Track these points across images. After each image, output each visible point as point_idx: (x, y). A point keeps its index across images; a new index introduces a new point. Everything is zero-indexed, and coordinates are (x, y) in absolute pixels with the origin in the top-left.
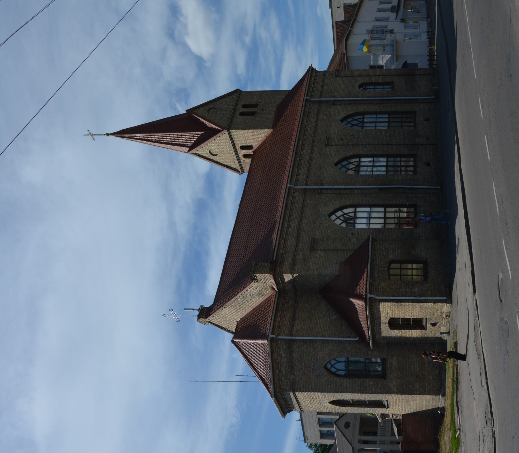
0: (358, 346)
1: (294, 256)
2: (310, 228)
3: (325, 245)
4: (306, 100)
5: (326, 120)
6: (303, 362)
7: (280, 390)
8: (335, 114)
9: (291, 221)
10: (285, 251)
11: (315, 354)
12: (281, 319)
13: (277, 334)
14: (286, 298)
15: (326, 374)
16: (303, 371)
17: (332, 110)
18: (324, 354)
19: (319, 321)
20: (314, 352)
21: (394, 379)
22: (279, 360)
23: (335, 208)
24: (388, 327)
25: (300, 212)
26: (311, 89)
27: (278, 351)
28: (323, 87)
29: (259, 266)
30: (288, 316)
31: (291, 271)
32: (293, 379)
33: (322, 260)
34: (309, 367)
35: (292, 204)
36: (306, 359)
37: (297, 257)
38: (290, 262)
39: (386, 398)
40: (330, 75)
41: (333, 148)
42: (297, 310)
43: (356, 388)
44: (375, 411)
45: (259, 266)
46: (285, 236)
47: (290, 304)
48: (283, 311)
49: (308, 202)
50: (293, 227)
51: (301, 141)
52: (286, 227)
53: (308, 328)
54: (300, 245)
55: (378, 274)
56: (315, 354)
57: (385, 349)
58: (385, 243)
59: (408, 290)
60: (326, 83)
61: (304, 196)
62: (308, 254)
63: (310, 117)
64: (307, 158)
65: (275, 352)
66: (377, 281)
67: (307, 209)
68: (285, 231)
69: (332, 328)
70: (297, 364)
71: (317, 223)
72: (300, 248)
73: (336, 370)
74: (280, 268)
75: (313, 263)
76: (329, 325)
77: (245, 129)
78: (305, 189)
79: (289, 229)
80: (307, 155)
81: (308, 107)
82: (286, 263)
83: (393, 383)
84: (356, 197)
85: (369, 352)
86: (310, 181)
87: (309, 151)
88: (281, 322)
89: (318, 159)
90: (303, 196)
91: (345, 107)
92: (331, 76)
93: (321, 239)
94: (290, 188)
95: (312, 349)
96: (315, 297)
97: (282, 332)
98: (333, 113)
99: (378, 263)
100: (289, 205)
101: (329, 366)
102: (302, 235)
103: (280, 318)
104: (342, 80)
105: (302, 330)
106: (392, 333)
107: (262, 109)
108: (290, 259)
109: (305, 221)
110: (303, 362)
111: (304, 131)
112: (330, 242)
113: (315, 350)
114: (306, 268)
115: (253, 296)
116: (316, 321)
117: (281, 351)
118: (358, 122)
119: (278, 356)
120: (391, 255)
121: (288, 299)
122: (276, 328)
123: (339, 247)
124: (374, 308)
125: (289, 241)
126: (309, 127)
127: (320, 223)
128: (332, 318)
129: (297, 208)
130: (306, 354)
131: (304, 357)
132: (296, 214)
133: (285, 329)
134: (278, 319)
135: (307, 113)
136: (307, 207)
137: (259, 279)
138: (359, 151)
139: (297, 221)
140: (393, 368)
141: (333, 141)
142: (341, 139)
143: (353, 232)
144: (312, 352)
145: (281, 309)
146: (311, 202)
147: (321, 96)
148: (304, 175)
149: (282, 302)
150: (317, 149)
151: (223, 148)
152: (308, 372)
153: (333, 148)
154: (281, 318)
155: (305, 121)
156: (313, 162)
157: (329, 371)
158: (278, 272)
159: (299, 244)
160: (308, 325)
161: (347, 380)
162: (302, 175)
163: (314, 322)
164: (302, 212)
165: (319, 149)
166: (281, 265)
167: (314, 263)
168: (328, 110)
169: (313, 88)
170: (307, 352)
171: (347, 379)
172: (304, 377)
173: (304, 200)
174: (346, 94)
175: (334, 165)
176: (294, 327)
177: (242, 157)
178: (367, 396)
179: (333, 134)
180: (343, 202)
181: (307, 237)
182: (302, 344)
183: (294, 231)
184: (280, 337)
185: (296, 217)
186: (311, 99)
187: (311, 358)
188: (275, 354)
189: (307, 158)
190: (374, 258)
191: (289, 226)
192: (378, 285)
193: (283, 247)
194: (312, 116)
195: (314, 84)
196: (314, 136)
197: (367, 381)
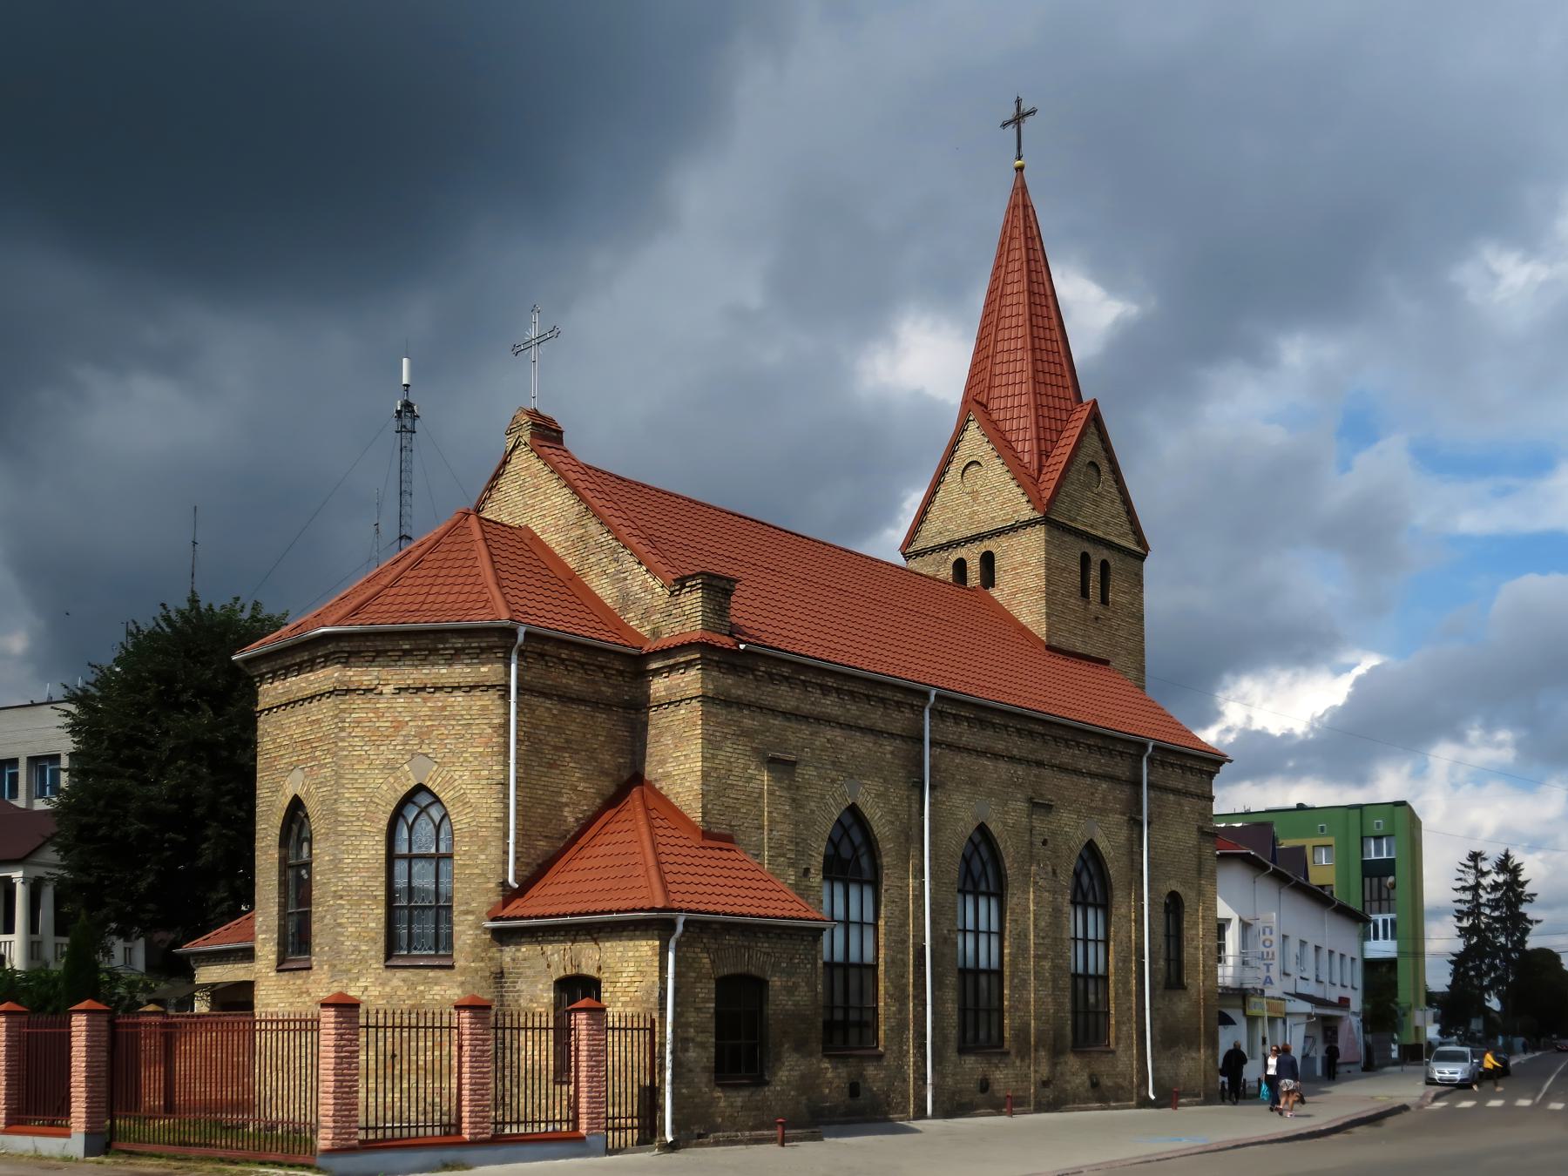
0: (492, 885)
1: (749, 705)
2: (822, 750)
3: (778, 793)
4: (1144, 746)
6: (436, 723)
7: (345, 652)
9: (839, 697)
10: (762, 676)
11: (461, 759)
12: (564, 660)
13: (523, 648)
14: (620, 679)
15: (399, 789)
16: (407, 722)
18: (464, 786)
19: (558, 772)
20: (468, 755)
21: (388, 989)
22: (441, 652)
23: (872, 823)
24: (562, 973)
25: (861, 723)
27: (471, 651)
28: (1176, 792)
29: (722, 600)
30: (572, 683)
31: (710, 695)
32: (381, 693)
33: (740, 783)
34: (422, 742)
36: (446, 732)
37: (745, 712)
38: (733, 691)
39: (321, 967)
42: (588, 709)
43: (354, 879)
44: (265, 932)
45: (722, 600)
46: (802, 677)
47: (603, 688)
48: (586, 667)
49: (888, 748)
50: (823, 701)
51: (1040, 729)
52: (824, 682)
53: (540, 740)
54: (776, 722)
55: (732, 947)
56: (461, 759)
57: (482, 964)
58: (809, 966)
59: (692, 1030)
61: (901, 736)
62: (754, 745)
63: (1101, 755)
65: (470, 640)
66: (713, 941)
68: (814, 680)
69: (539, 811)
70: (429, 704)
71: (834, 773)
72: (771, 721)
73: (410, 822)
74: (717, 662)
75: (732, 760)
76: (548, 802)
77: (1048, 568)
78: (922, 740)
79: (818, 691)
82: (730, 681)
83: (373, 988)
85: (471, 918)
87: (1015, 752)
88: (555, 660)
89: (995, 776)
90: (904, 734)
93: (794, 781)
94: (926, 695)
95: (481, 750)
96: (621, 760)
97: (528, 662)
99: (759, 945)
100: (881, 693)
101: (424, 799)
102: (803, 727)
103: (567, 660)
105: (534, 721)
106: (540, 986)
107: (1097, 618)
108: (740, 692)
109: (839, 739)
110: (436, 723)
112: (787, 808)
113: (476, 758)
114: (718, 739)
115: (618, 579)
116: (559, 763)
117: (472, 659)
119: (456, 650)
120: (778, 983)
121: (616, 682)
122: (541, 646)
123: (774, 833)
124: (638, 933)
125: (789, 689)
126: (1077, 752)
127: (833, 781)
128: (567, 809)
129: (872, 716)
130: (463, 732)
131: (453, 726)
132: (858, 713)
133: (536, 671)
134: (564, 654)
136: (875, 743)
137: (682, 598)
139: (839, 713)
140: (422, 988)
143: (811, 875)
144: (470, 750)
145: (591, 662)
146: (889, 756)
147: (1151, 786)
149: (609, 665)
150: (1020, 773)
151: (988, 502)
152: (405, 736)
154: (567, 663)
155: (1091, 742)
157: (408, 798)
158: (709, 657)
159: (780, 719)
160: (549, 739)
161: (380, 852)
162: (955, 729)
163: (555, 757)
164: (860, 729)
165: (1020, 781)
166: (725, 666)
167: (731, 762)
169: (1172, 765)
170: (469, 736)
171: (384, 852)
172: (388, 724)
173: (892, 734)
176: (541, 700)
177: (957, 557)
178: (326, 911)
181: (797, 741)
182: (496, 721)
183: (812, 704)
184: (514, 657)
185: (848, 710)
186: (1145, 759)
187: (449, 746)
188: (462, 641)
190: (770, 935)
191: (825, 690)
192: (702, 945)
193: (774, 671)
195: (1181, 767)
196: (1053, 766)
197: (379, 911)
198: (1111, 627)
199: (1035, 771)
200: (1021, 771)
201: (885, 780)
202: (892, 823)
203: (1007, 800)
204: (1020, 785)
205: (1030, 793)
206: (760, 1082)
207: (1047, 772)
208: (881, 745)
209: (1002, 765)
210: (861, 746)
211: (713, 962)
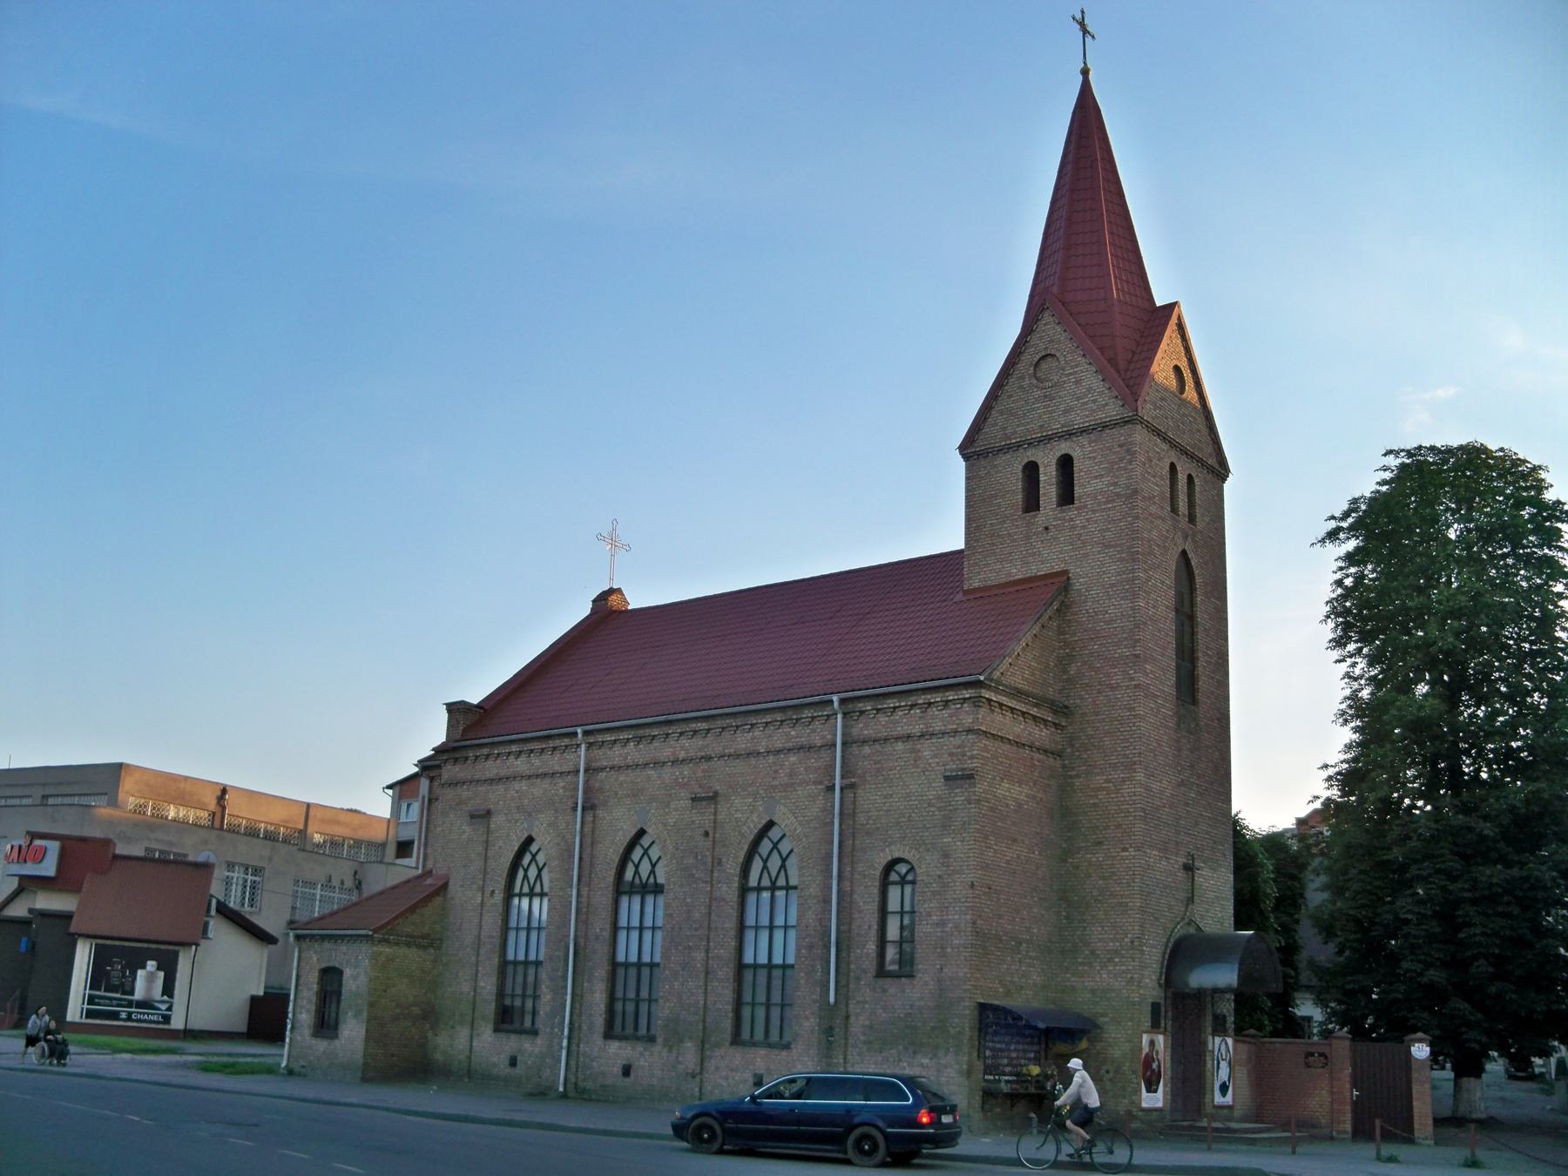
5: (774, 778)
8: (793, 801)
17: (808, 788)
26: (890, 701)
35: (555, 749)
40: (955, 751)
41: (685, 816)
51: (703, 725)
54: (483, 788)
60: (919, 746)
64: (665, 754)
67: (547, 786)
80: (671, 750)
81: (815, 714)
82: (457, 769)
84: (561, 894)
86: (606, 776)
89: (659, 782)
91: (817, 825)
92: (951, 754)
98: (799, 792)
104: (931, 797)
111: (734, 724)
118: (774, 875)
127: (516, 821)
135: (795, 717)
138: (672, 887)
141: (703, 811)
142: (707, 834)
146: (561, 791)
148: (621, 758)
150: (685, 773)
153: (685, 816)
156: (653, 772)
162: (621, 752)
165: (686, 780)
168: (811, 776)
174: (871, 822)
175: (639, 827)
179: (729, 808)
180: (554, 864)
183: (508, 767)
189: (665, 754)
194: (793, 733)
198: (1073, 528)
199: (704, 766)
200: (686, 770)
201: (556, 811)
202: (558, 844)
203: (669, 802)
204: (685, 784)
205: (697, 789)
206: (336, 1037)
207: (715, 764)
208: (555, 785)
209: (668, 771)
210: (539, 789)
211: (318, 960)
